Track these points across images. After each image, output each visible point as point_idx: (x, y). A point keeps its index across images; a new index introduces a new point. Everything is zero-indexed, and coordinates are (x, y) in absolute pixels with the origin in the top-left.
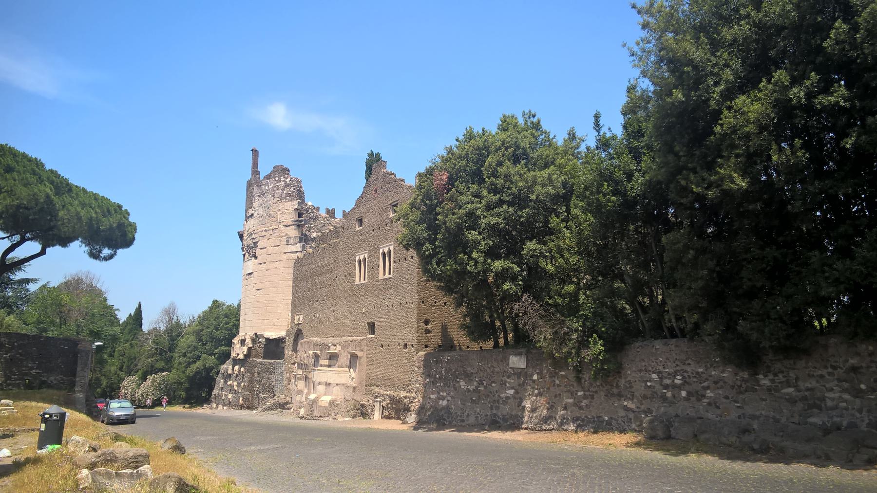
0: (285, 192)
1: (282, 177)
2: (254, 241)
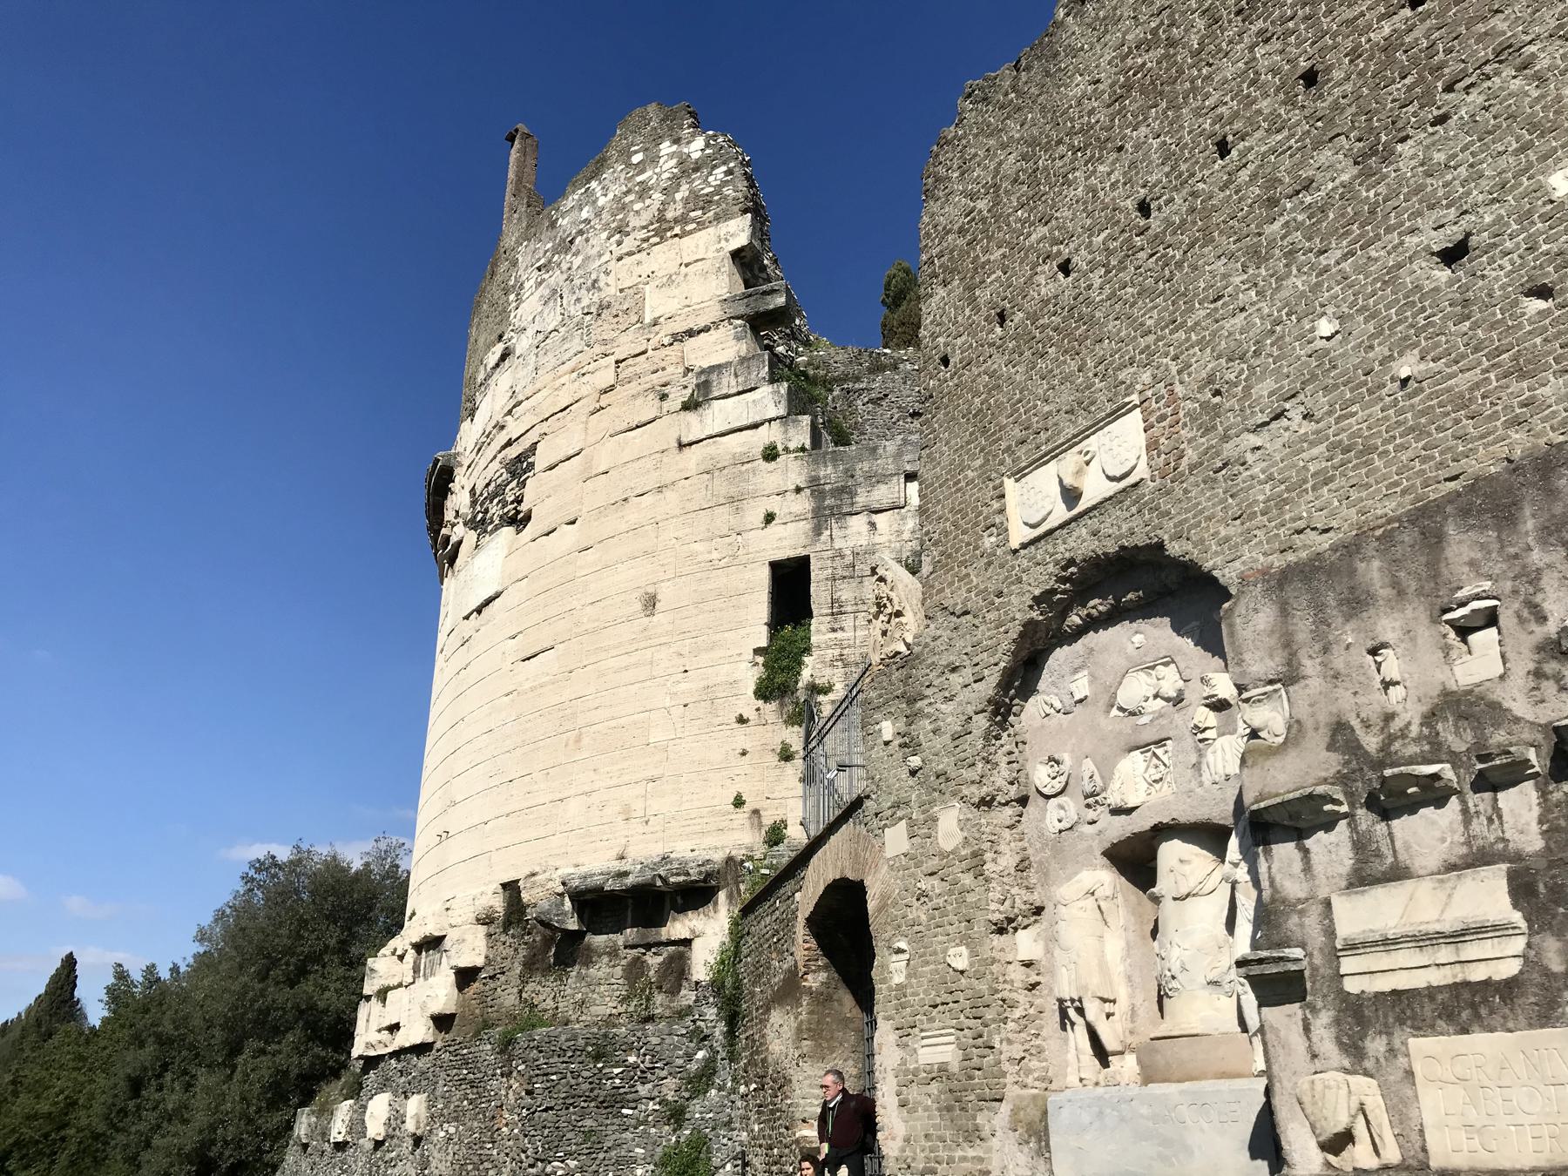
0: (678, 196)
1: (667, 143)
2: (513, 452)
